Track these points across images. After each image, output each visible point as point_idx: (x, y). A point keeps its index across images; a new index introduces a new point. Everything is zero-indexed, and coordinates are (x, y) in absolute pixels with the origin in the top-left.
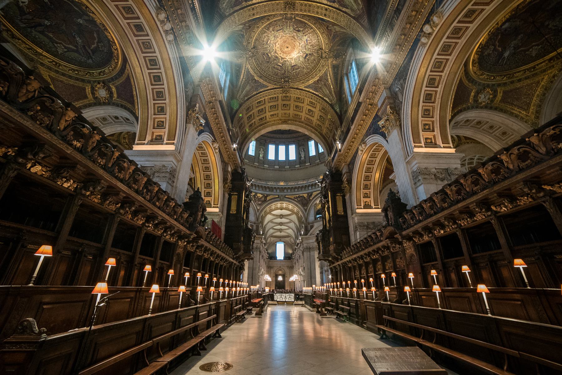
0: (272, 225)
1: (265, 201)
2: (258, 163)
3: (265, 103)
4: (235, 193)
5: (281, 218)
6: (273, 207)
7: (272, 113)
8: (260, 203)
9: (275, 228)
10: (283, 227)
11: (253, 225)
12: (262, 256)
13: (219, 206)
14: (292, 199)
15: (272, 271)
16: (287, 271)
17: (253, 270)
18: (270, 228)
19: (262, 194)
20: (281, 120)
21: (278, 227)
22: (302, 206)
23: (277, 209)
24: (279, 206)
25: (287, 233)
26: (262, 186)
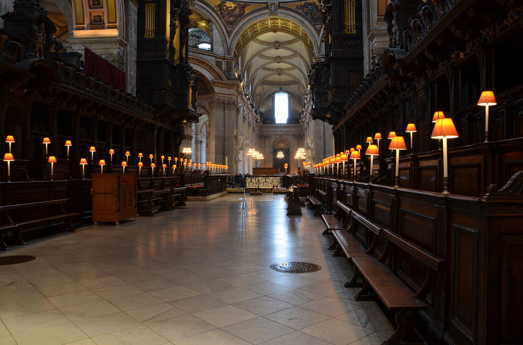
0: (264, 61)
1: (241, 15)
5: (277, 49)
6: (259, 27)
9: (268, 66)
10: (282, 65)
11: (221, 62)
12: (244, 118)
13: (117, 24)
14: (292, 10)
15: (269, 143)
17: (224, 141)
18: (259, 69)
21: (276, 65)
22: (311, 23)
23: (266, 30)
24: (269, 25)
25: (292, 76)
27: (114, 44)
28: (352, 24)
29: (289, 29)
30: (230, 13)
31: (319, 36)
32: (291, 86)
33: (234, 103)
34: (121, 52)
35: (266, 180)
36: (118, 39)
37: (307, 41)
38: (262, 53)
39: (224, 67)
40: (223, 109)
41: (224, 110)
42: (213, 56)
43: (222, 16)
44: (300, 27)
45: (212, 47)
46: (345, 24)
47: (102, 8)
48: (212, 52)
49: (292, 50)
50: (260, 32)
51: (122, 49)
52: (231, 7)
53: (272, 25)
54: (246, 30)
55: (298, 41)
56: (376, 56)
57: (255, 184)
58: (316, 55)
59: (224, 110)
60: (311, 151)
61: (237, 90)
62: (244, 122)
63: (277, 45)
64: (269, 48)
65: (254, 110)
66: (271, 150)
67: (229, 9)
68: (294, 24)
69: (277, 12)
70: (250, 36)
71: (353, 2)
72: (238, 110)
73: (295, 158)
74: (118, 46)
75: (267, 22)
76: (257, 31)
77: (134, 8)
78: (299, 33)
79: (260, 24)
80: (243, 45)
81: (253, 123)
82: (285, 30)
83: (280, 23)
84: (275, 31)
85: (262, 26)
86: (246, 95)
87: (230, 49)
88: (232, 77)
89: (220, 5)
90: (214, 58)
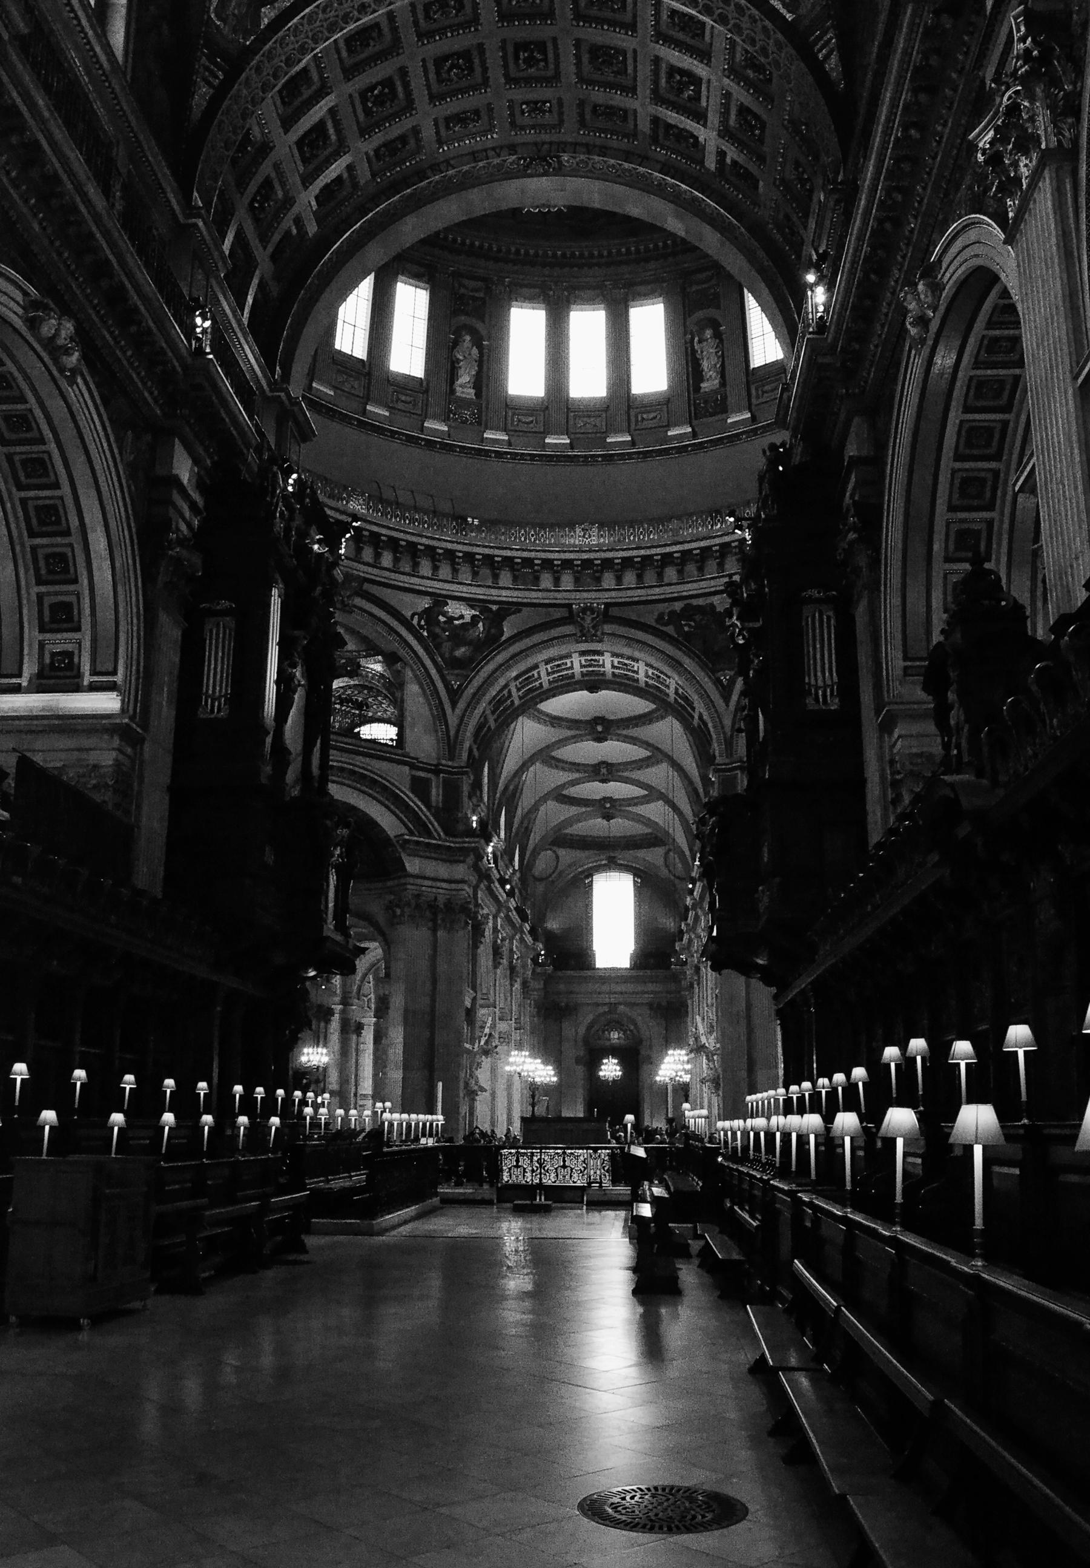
1: (492, 642)
2: (446, 420)
3: (396, 42)
4: (225, 604)
5: (600, 739)
7: (452, 106)
8: (461, 652)
9: (574, 791)
10: (617, 789)
11: (427, 781)
13: (119, 678)
15: (575, 1030)
16: (649, 1027)
17: (432, 1026)
18: (544, 799)
19: (470, 602)
20: (512, 148)
21: (595, 789)
22: (703, 666)
25: (648, 822)
26: (469, 557)
27: (106, 737)
28: (829, 682)
29: (637, 680)
30: (459, 633)
31: (727, 705)
32: (641, 853)
33: (464, 909)
34: (127, 762)
35: (564, 1161)
36: (118, 721)
37: (693, 717)
38: (553, 754)
39: (436, 794)
40: (430, 924)
41: (434, 930)
42: (405, 763)
43: (433, 644)
44: (669, 677)
45: (400, 734)
46: (807, 680)
47: (78, 629)
48: (400, 752)
49: (647, 745)
50: (549, 690)
51: (129, 750)
52: (462, 617)
53: (584, 670)
54: (506, 686)
55: (663, 718)
56: (901, 781)
57: (528, 1174)
58: (718, 760)
59: (434, 930)
60: (708, 1059)
61: (476, 868)
62: (496, 964)
63: (600, 728)
64: (574, 737)
65: (527, 927)
66: (582, 1053)
67: (456, 622)
68: (652, 667)
69: (599, 633)
70: (517, 702)
71: (829, 618)
72: (478, 931)
73: (658, 1079)
74: (116, 742)
75: (568, 661)
76: (537, 689)
77: (171, 631)
78: (668, 695)
79: (548, 666)
80: (498, 728)
81: (524, 966)
82: (624, 684)
83: (608, 663)
84: (593, 688)
85: (553, 673)
86: (503, 882)
87: (455, 742)
88: (461, 827)
89: (426, 611)
90: (406, 769)
